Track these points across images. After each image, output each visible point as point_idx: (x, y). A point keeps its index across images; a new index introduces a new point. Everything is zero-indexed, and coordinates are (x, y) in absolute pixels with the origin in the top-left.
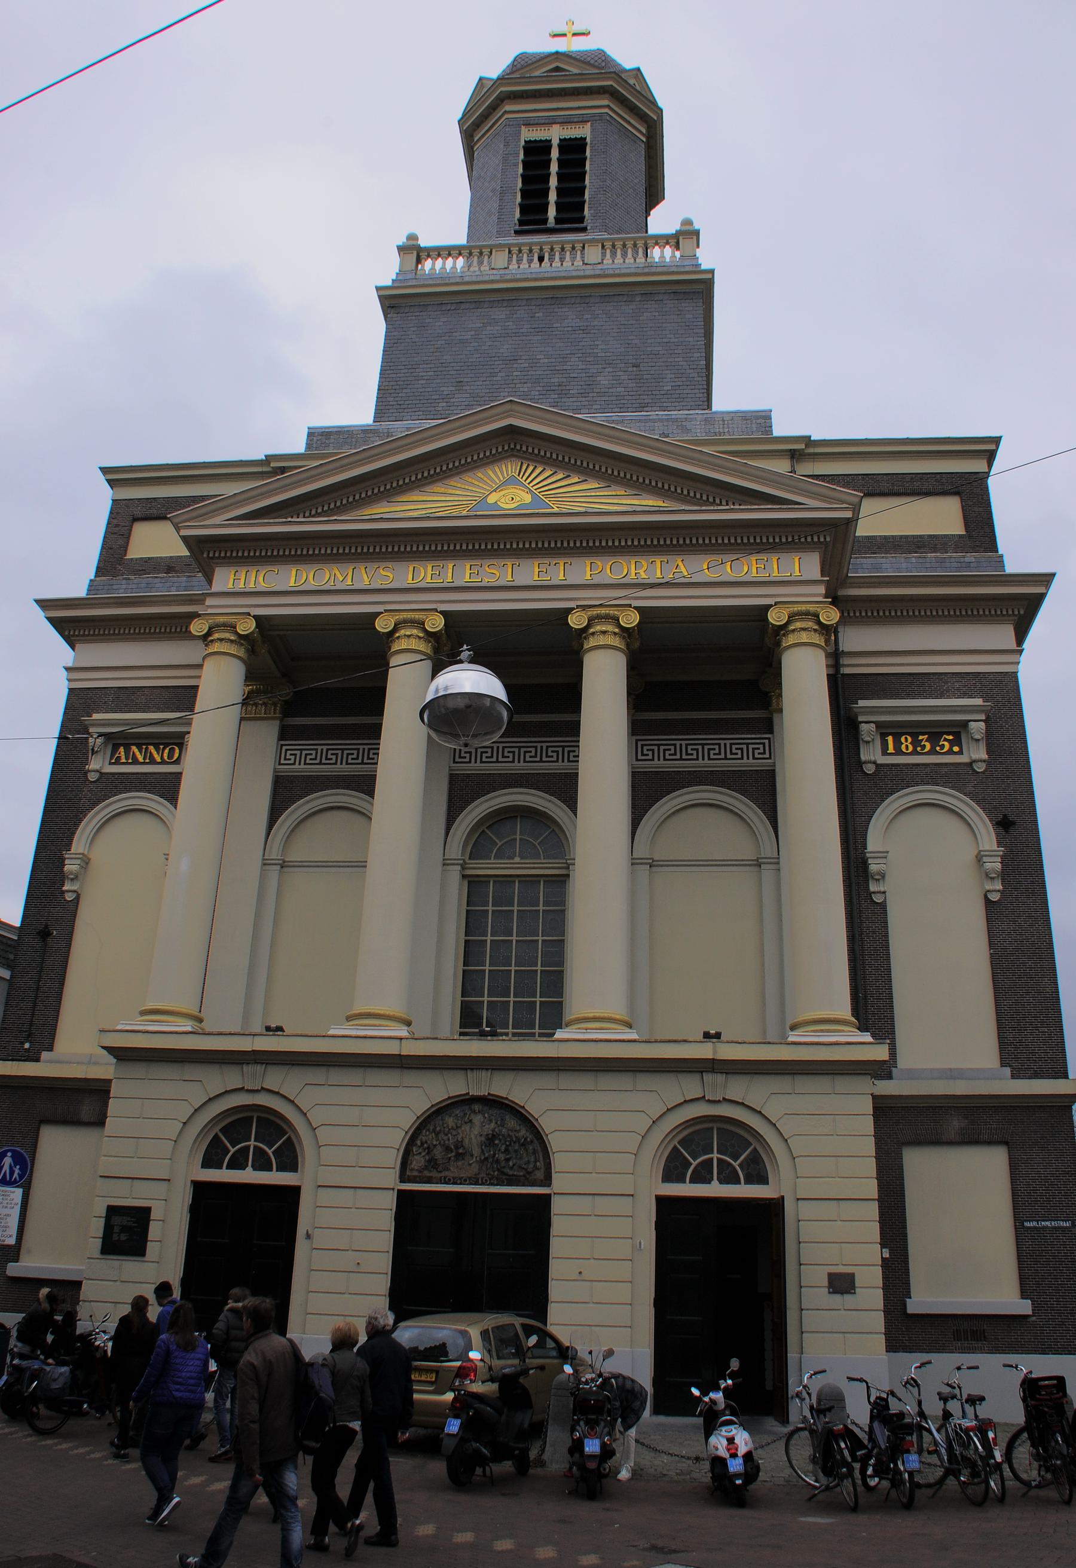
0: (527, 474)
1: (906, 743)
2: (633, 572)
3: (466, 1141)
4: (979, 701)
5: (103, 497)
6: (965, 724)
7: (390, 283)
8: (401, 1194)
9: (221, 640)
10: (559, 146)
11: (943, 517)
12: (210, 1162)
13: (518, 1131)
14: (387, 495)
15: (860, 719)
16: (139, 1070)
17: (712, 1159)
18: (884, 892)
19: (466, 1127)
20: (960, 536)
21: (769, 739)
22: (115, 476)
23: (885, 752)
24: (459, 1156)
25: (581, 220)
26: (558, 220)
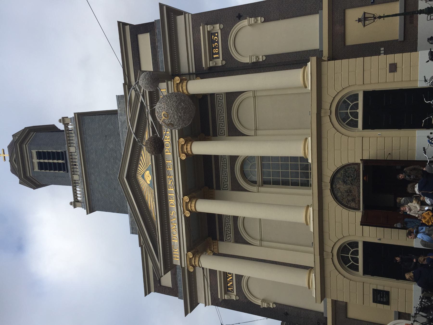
1: (215, 51)
2: (168, 140)
3: (345, 189)
4: (201, 27)
5: (154, 295)
6: (209, 32)
7: (85, 210)
9: (194, 262)
10: (39, 159)
11: (145, 40)
12: (356, 269)
13: (342, 173)
15: (209, 66)
16: (328, 291)
17: (350, 112)
18: (262, 56)
19: (341, 190)
20: (150, 35)
22: (147, 291)
23: (218, 58)
24: (351, 191)
25: (62, 152)
26: (63, 160)
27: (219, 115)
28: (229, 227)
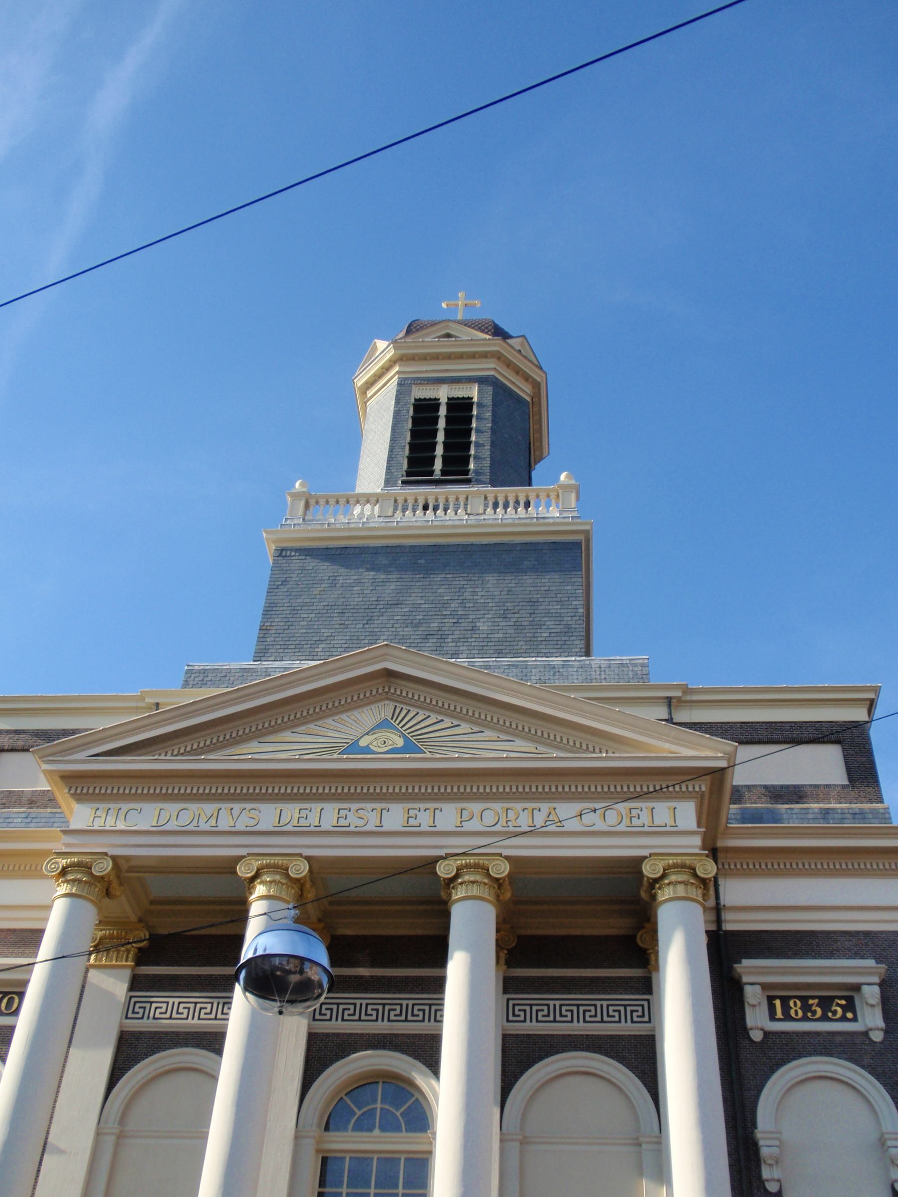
0: (400, 718)
1: (796, 1007)
4: (870, 963)
6: (857, 988)
10: (447, 404)
11: (824, 765)
14: (258, 735)
15: (745, 979)
18: (778, 1181)
20: (843, 787)
21: (648, 1000)
23: (772, 1017)
25: (467, 472)
26: (443, 473)
27: (578, 1006)
28: (172, 1011)
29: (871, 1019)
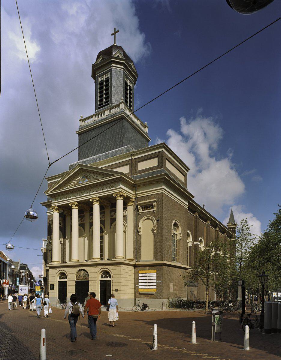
8: (76, 281)
23: (142, 211)
29: (155, 209)
